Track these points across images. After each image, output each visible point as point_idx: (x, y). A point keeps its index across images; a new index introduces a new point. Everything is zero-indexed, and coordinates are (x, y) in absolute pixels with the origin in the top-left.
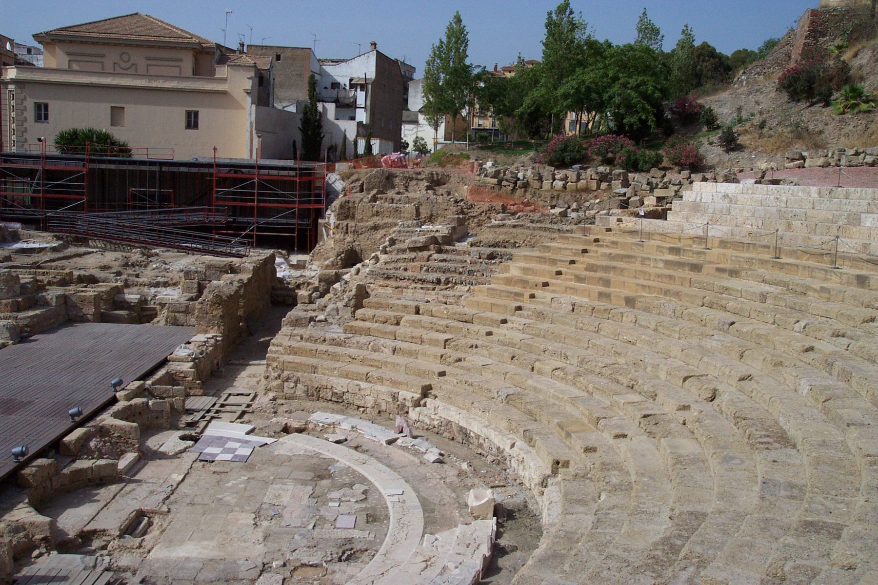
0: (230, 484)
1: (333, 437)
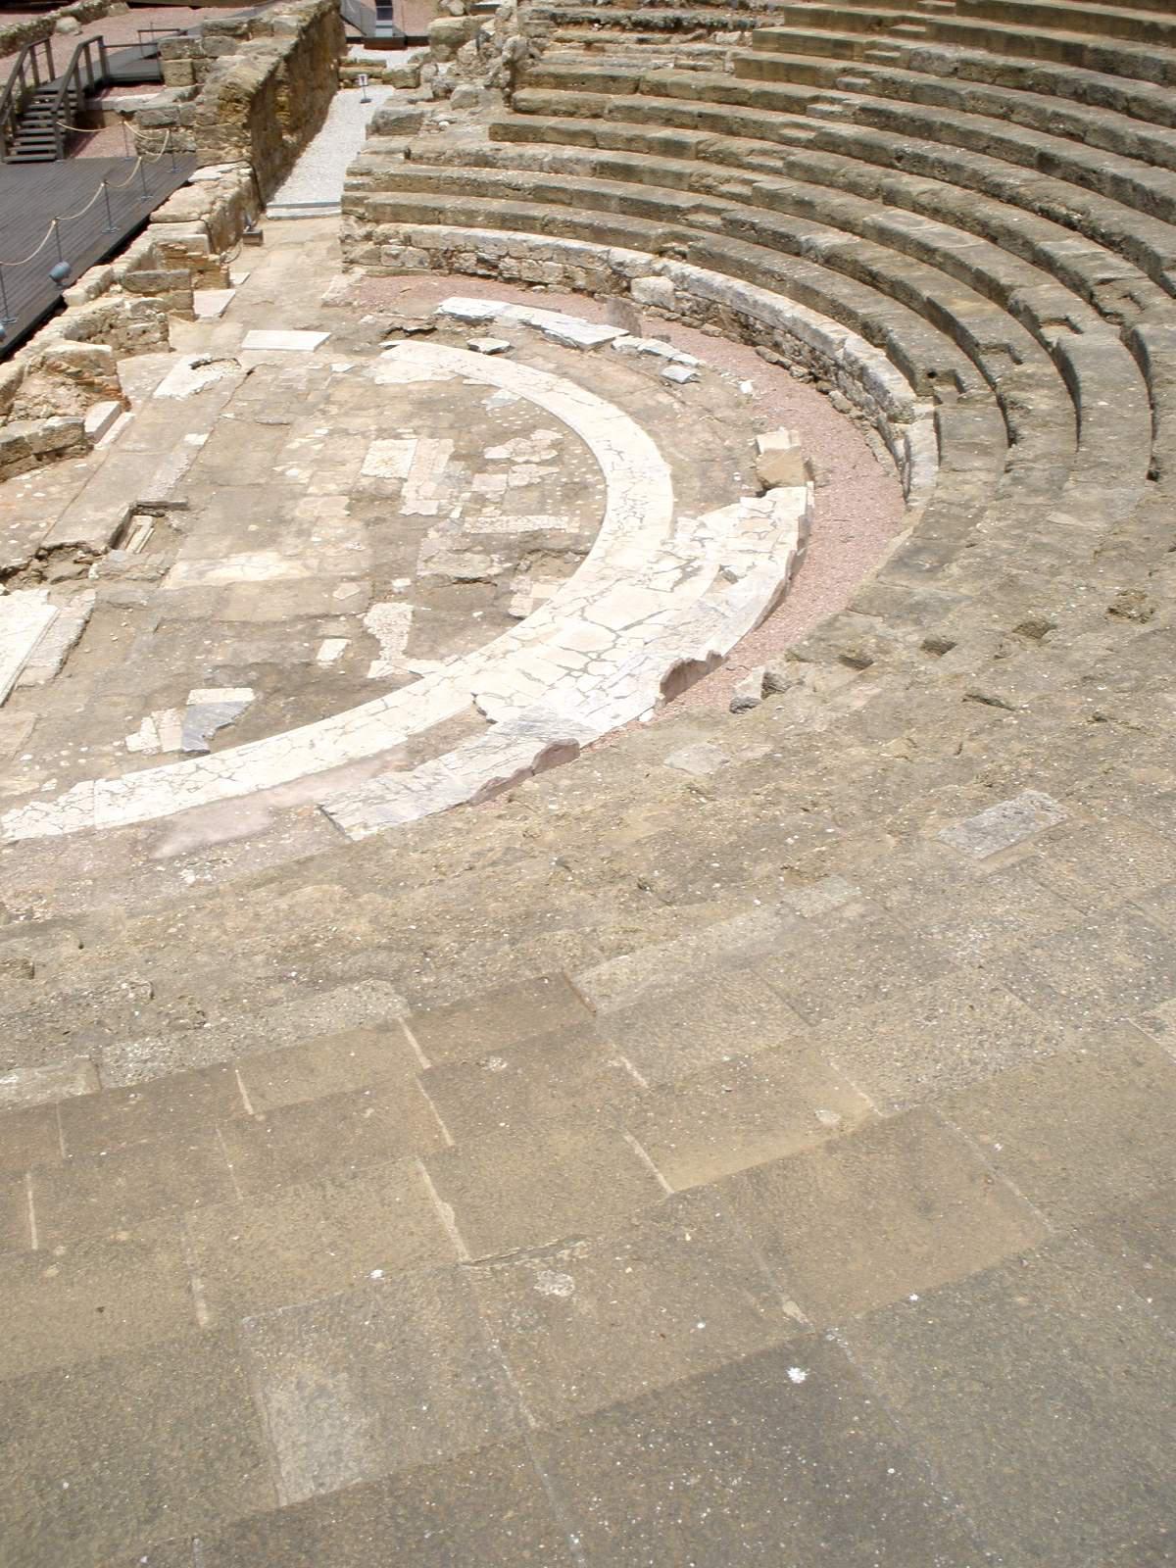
0: (295, 445)
1: (486, 344)
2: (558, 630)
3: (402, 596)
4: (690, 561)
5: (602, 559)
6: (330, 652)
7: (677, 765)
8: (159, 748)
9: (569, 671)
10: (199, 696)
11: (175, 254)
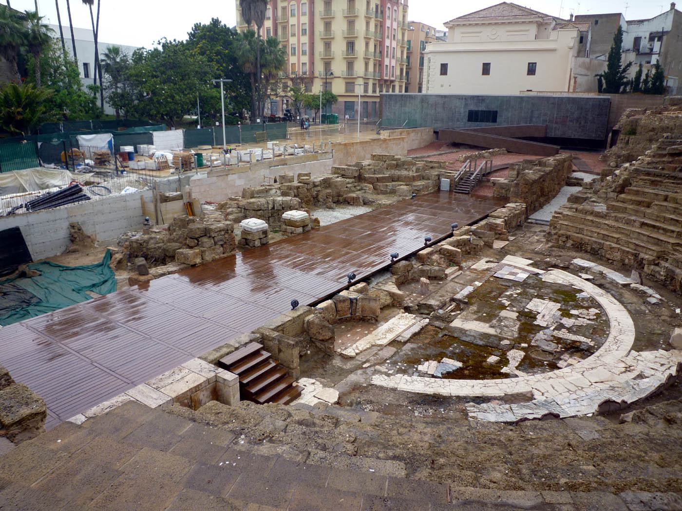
0: (508, 293)
2: (572, 376)
3: (523, 349)
4: (630, 366)
5: (598, 357)
6: (492, 359)
7: (579, 434)
8: (427, 372)
9: (569, 391)
10: (445, 360)
11: (492, 227)
